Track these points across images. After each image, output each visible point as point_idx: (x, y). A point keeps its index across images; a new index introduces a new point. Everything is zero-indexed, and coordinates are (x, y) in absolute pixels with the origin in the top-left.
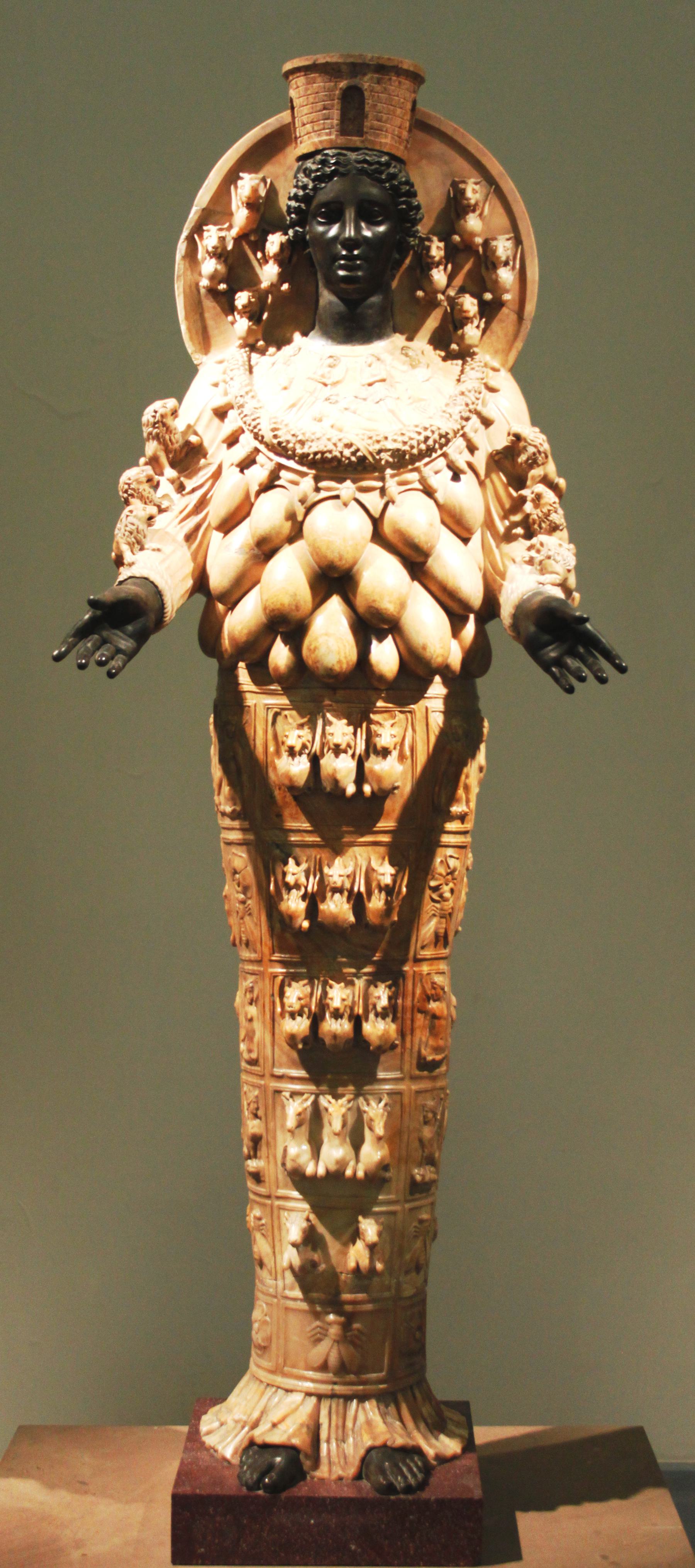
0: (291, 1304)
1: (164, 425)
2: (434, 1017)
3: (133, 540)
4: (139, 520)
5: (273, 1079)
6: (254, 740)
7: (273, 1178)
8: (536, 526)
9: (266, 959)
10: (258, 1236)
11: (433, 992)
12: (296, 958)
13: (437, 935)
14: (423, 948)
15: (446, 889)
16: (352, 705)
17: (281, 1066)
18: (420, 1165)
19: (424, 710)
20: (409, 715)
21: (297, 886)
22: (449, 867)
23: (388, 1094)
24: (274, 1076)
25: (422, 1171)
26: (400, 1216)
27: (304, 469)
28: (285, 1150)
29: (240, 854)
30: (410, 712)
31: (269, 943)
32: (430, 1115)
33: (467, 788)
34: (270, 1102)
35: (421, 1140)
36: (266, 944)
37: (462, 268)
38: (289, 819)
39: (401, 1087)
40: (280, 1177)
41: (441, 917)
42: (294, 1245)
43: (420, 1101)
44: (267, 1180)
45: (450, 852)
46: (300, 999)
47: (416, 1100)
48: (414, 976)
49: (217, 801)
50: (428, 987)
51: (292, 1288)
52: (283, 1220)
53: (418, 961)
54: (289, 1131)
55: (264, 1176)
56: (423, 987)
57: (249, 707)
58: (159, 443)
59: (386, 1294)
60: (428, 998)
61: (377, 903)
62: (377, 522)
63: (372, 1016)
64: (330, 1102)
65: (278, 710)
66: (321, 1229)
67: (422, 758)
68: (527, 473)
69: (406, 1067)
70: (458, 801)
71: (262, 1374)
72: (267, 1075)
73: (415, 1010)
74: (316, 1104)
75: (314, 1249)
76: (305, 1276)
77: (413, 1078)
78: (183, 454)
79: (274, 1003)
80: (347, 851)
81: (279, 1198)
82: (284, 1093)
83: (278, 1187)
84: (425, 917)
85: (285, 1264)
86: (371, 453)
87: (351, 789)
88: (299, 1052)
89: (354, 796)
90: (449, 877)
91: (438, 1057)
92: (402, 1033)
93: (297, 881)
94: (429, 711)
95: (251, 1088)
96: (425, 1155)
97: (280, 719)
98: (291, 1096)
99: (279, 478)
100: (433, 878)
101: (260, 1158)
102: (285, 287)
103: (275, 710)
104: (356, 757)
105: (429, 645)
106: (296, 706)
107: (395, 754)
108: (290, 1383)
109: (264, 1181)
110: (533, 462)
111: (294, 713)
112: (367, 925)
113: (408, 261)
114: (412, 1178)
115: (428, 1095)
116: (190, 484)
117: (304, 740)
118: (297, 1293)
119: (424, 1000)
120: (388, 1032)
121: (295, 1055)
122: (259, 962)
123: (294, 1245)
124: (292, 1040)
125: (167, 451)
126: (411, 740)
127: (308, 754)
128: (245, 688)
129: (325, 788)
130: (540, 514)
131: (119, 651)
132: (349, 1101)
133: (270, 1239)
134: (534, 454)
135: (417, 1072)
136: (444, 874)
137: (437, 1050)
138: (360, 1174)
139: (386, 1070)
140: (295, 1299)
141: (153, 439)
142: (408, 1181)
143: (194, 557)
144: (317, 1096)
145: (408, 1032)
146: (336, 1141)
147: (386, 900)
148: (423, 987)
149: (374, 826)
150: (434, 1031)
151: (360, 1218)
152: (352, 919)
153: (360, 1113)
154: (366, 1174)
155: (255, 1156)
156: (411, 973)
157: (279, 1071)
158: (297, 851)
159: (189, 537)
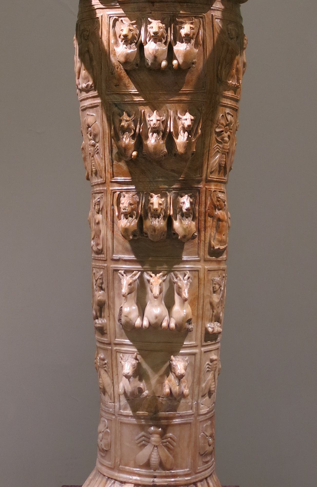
0: (125, 420)
2: (219, 220)
5: (112, 262)
6: (101, 38)
7: (112, 331)
9: (108, 181)
10: (102, 372)
11: (218, 203)
12: (128, 179)
13: (220, 166)
14: (211, 173)
15: (226, 135)
17: (118, 253)
18: (211, 321)
19: (211, 17)
21: (128, 129)
22: (228, 121)
23: (189, 271)
24: (113, 260)
25: (212, 325)
26: (198, 357)
28: (121, 310)
29: (91, 114)
30: (201, 17)
31: (110, 170)
32: (217, 286)
33: (237, 70)
34: (111, 278)
35: (211, 304)
36: (108, 172)
38: (124, 87)
39: (198, 266)
40: (117, 329)
41: (223, 154)
42: (127, 377)
43: (211, 276)
44: (108, 333)
45: (228, 111)
46: (130, 204)
47: (208, 276)
48: (206, 191)
49: (77, 83)
50: (215, 200)
51: (125, 409)
52: (120, 360)
53: (208, 181)
54: (124, 296)
55: (106, 330)
56: (212, 199)
57: (98, 18)
59: (190, 412)
60: (215, 207)
61: (182, 139)
63: (178, 216)
64: (151, 276)
65: (117, 18)
66: (145, 366)
67: (209, 47)
69: (202, 253)
70: (232, 77)
71: (104, 470)
72: (109, 260)
73: (207, 214)
74: (141, 278)
75: (140, 380)
76: (134, 399)
77: (206, 261)
79: (113, 210)
80: (162, 107)
81: (116, 344)
82: (120, 271)
83: (115, 338)
84: (213, 152)
85: (121, 390)
87: (164, 63)
88: (130, 241)
89: (166, 67)
90: (227, 127)
91: (222, 247)
92: (199, 231)
93: (129, 125)
94: (214, 18)
95: (98, 270)
96: (214, 314)
98: (124, 273)
100: (218, 127)
101: (104, 317)
103: (115, 17)
104: (168, 43)
106: (128, 15)
107: (193, 41)
108: (124, 477)
109: (106, 333)
111: (127, 19)
112: (176, 155)
114: (206, 330)
115: (215, 273)
117: (134, 32)
118: (129, 412)
119: (212, 208)
120: (190, 227)
121: (128, 245)
122: (103, 184)
123: (127, 377)
124: (126, 230)
126: (202, 35)
127: (136, 43)
128: (96, 7)
129: (148, 64)
132: (164, 276)
133: (110, 373)
135: (209, 257)
136: (225, 124)
137: (221, 242)
138: (172, 325)
139: (188, 254)
140: (127, 416)
142: (204, 332)
144: (142, 272)
145: (203, 229)
146: (156, 302)
147: (188, 137)
148: (212, 199)
149: (180, 90)
150: (219, 230)
151: (172, 357)
152: (166, 150)
153: (172, 283)
154: (176, 325)
155: (101, 316)
156: (205, 189)
157: (116, 256)
158: (129, 108)
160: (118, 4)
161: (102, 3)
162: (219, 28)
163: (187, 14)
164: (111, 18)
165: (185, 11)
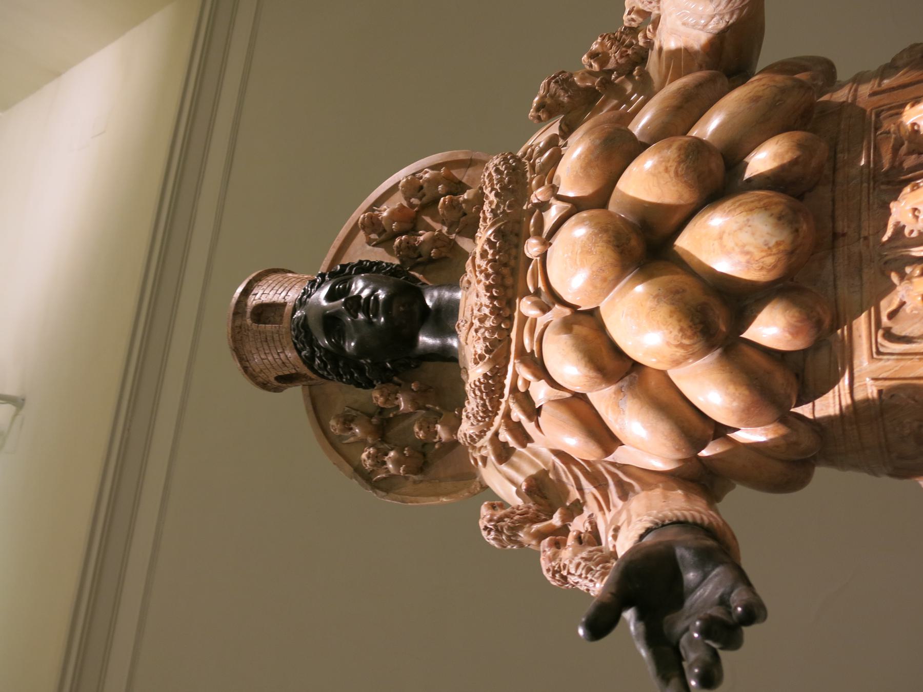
1: (501, 519)
3: (598, 568)
4: (575, 555)
8: (630, 52)
16: (864, 204)
19: (876, 98)
20: (883, 115)
27: (516, 314)
30: (878, 115)
37: (428, 224)
57: (880, 392)
58: (520, 528)
62: (576, 206)
65: (880, 332)
68: (579, 89)
78: (543, 501)
86: (492, 225)
97: (898, 329)
99: (532, 351)
102: (413, 386)
103: (880, 340)
105: (751, 94)
110: (565, 82)
113: (417, 275)
116: (575, 495)
125: (534, 520)
128: (846, 400)
130: (614, 48)
131: (723, 602)
134: (556, 82)
141: (516, 535)
143: (646, 486)
159: (625, 492)
160: (839, 331)
161: (836, 381)
162: (908, 75)
163: (869, 143)
164: (882, 350)
165: (861, 151)
